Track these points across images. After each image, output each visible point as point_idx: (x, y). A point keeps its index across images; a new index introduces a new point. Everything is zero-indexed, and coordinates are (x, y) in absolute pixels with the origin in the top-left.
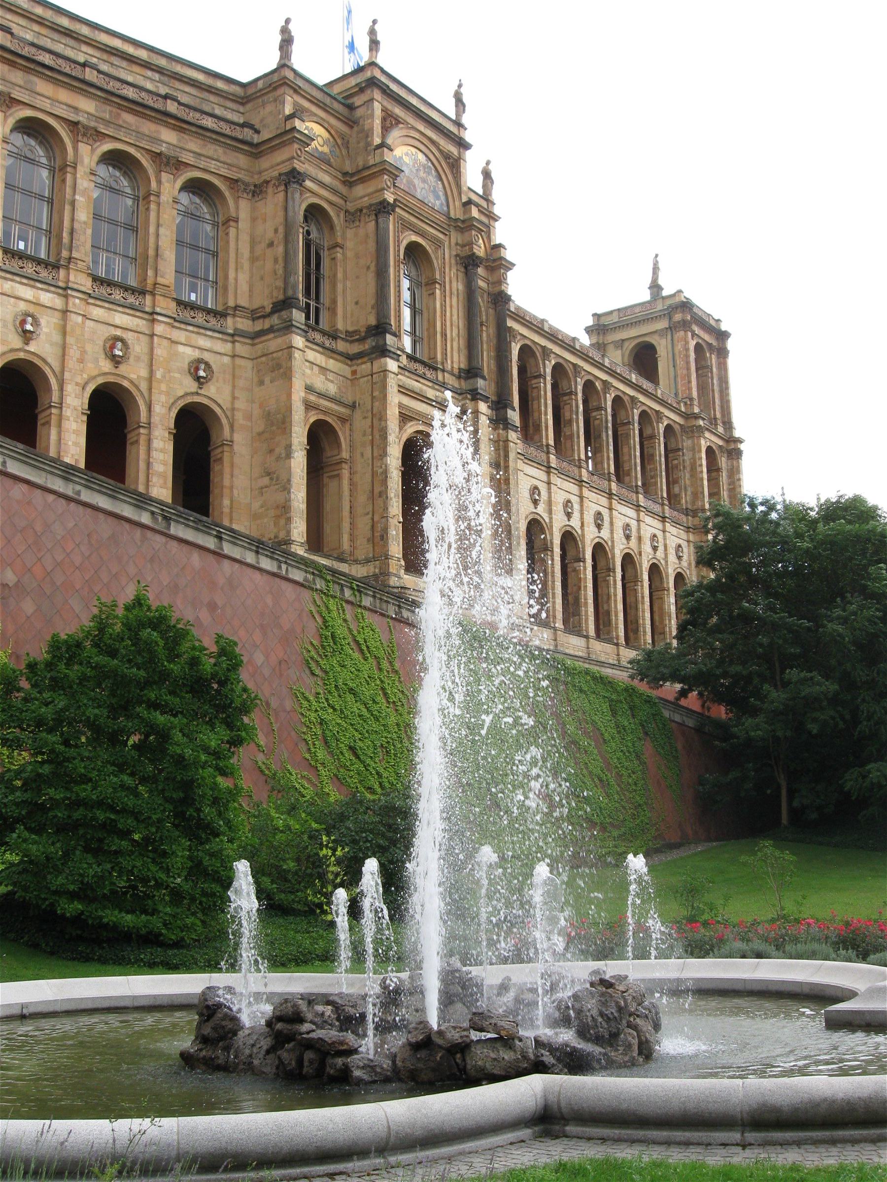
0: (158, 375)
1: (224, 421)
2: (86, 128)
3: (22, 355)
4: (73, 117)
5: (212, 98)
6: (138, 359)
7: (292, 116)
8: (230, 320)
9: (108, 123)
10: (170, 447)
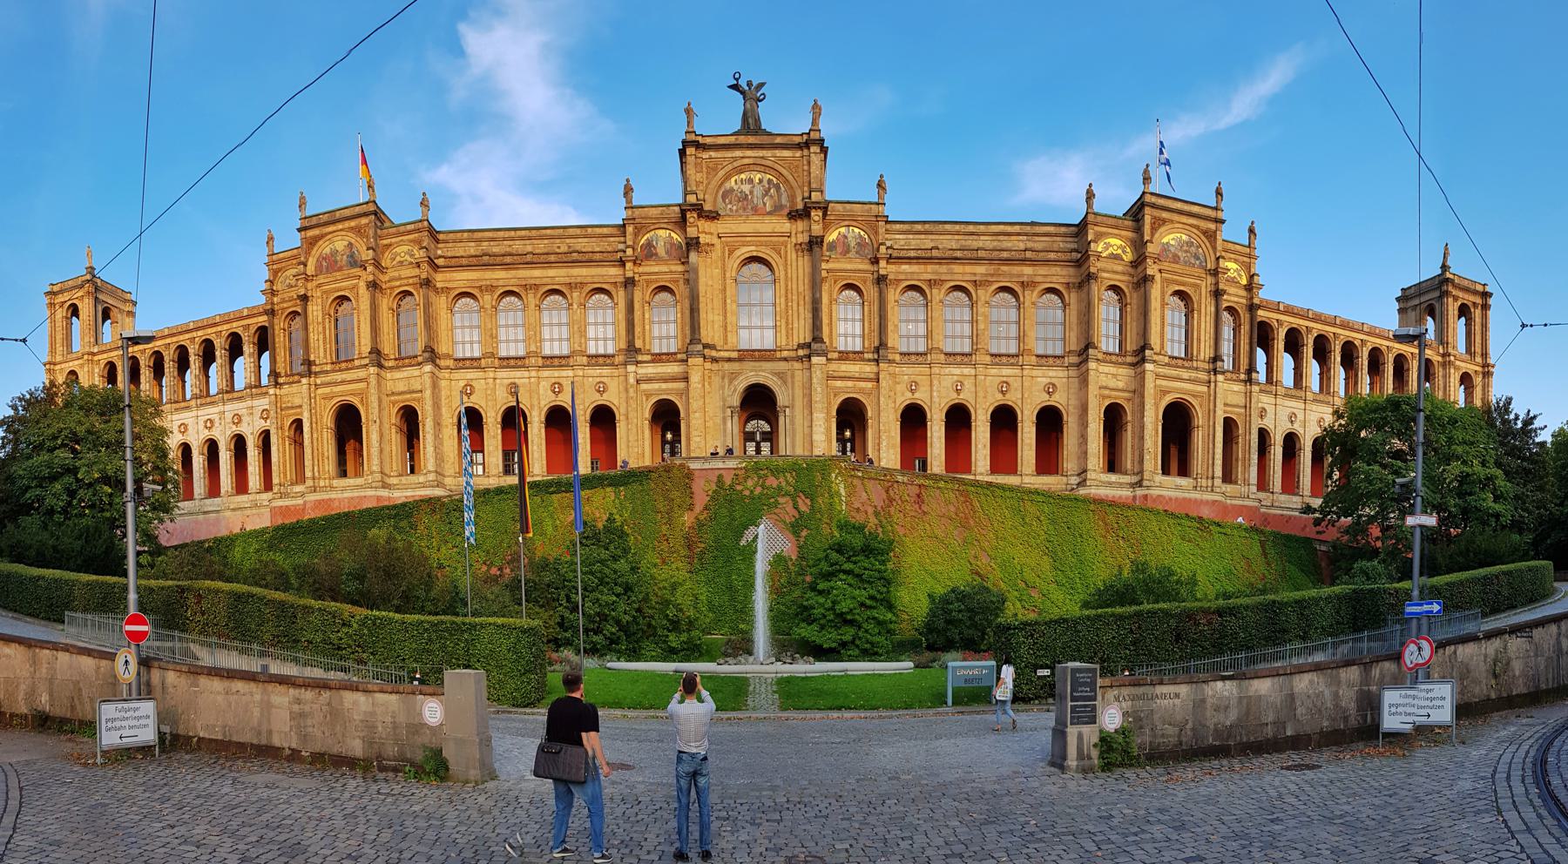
0: (1026, 396)
1: (1064, 412)
2: (980, 281)
3: (957, 401)
4: (974, 279)
6: (1016, 389)
9: (992, 275)
10: (1034, 429)
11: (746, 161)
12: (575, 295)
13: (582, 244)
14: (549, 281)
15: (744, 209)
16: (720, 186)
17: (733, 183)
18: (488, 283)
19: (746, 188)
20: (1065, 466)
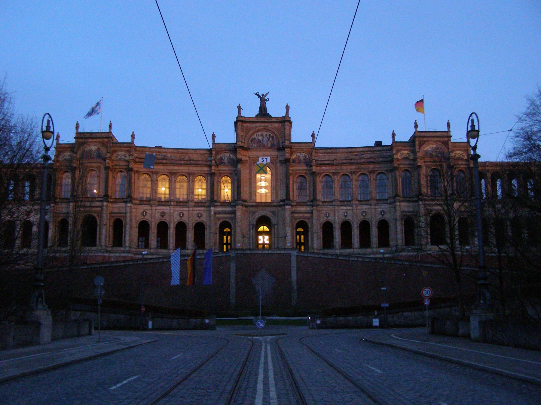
0: (373, 216)
2: (353, 172)
3: (345, 220)
4: (351, 171)
5: (384, 152)
7: (394, 154)
8: (389, 200)
11: (261, 128)
12: (191, 178)
13: (194, 157)
14: (180, 171)
15: (260, 146)
16: (250, 137)
17: (255, 136)
18: (156, 170)
19: (260, 138)
20: (390, 243)
